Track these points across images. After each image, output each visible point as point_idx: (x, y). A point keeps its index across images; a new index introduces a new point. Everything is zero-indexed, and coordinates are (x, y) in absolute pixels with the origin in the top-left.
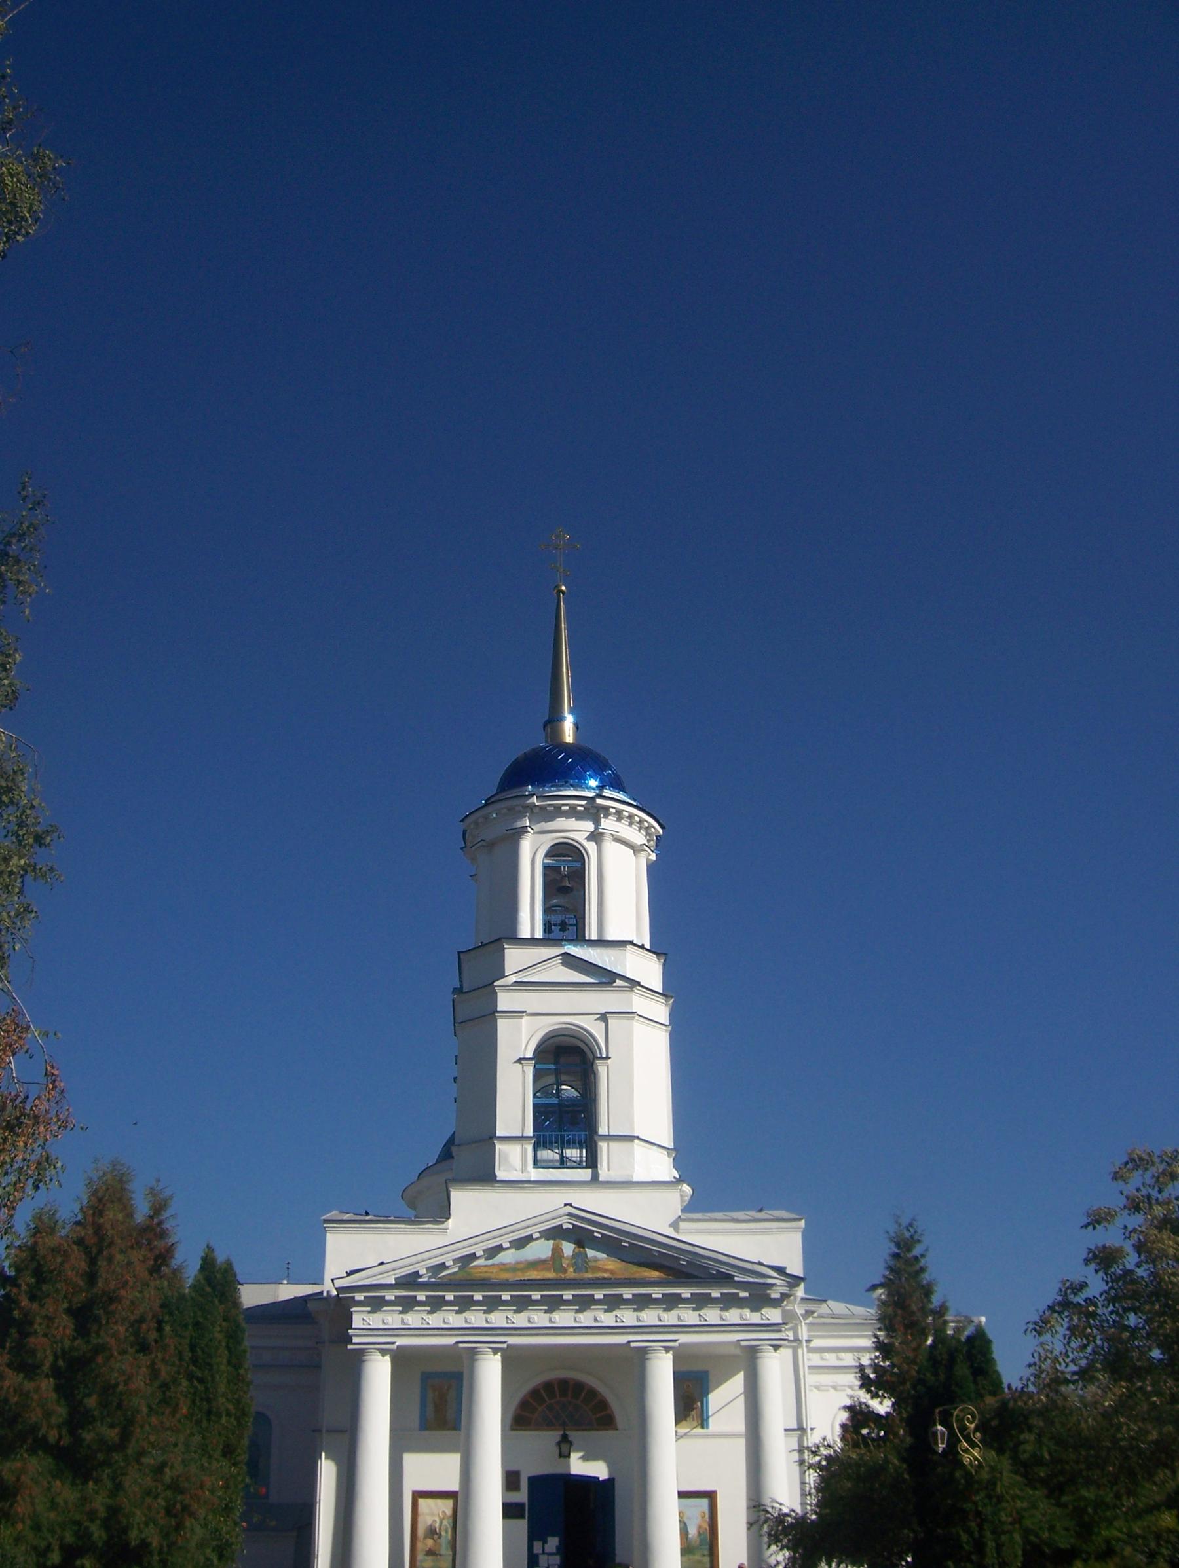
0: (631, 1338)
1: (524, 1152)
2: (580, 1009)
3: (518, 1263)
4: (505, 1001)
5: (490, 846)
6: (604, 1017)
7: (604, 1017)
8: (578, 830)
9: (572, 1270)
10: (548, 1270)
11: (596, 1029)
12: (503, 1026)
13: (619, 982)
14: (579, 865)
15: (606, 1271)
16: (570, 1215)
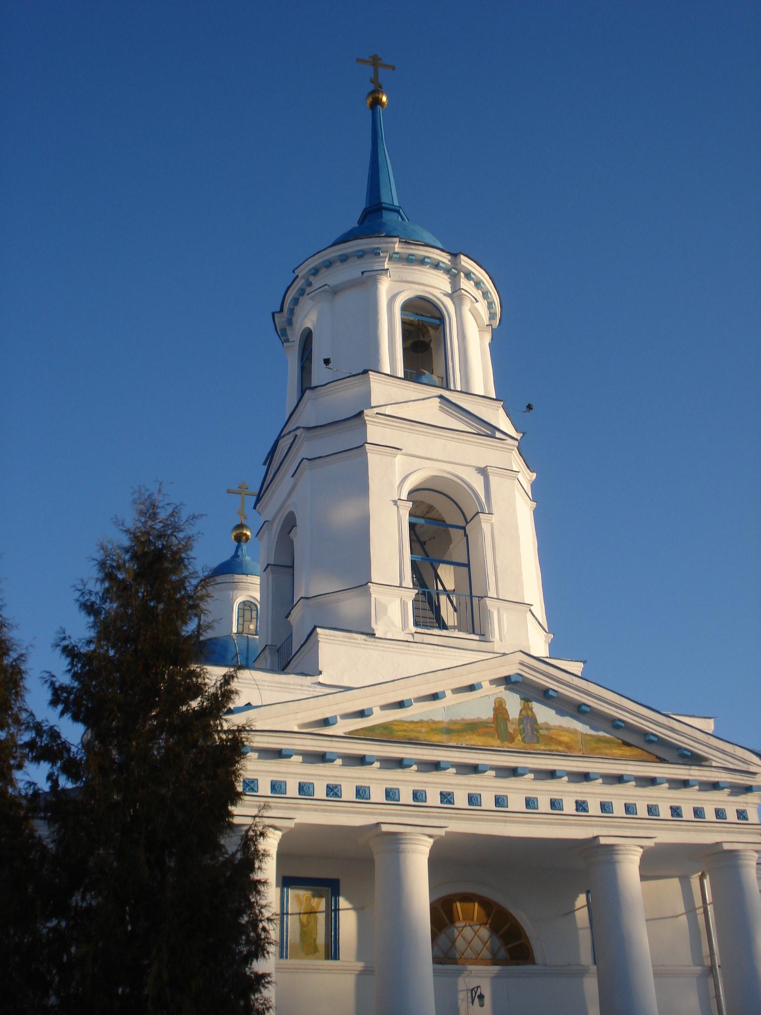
0: (595, 832)
1: (403, 605)
2: (456, 458)
3: (453, 722)
4: (375, 432)
5: (335, 291)
6: (483, 471)
7: (483, 471)
8: (435, 284)
9: (520, 738)
10: (492, 736)
11: (477, 483)
12: (374, 459)
13: (498, 435)
14: (438, 322)
15: (560, 743)
16: (522, 664)
